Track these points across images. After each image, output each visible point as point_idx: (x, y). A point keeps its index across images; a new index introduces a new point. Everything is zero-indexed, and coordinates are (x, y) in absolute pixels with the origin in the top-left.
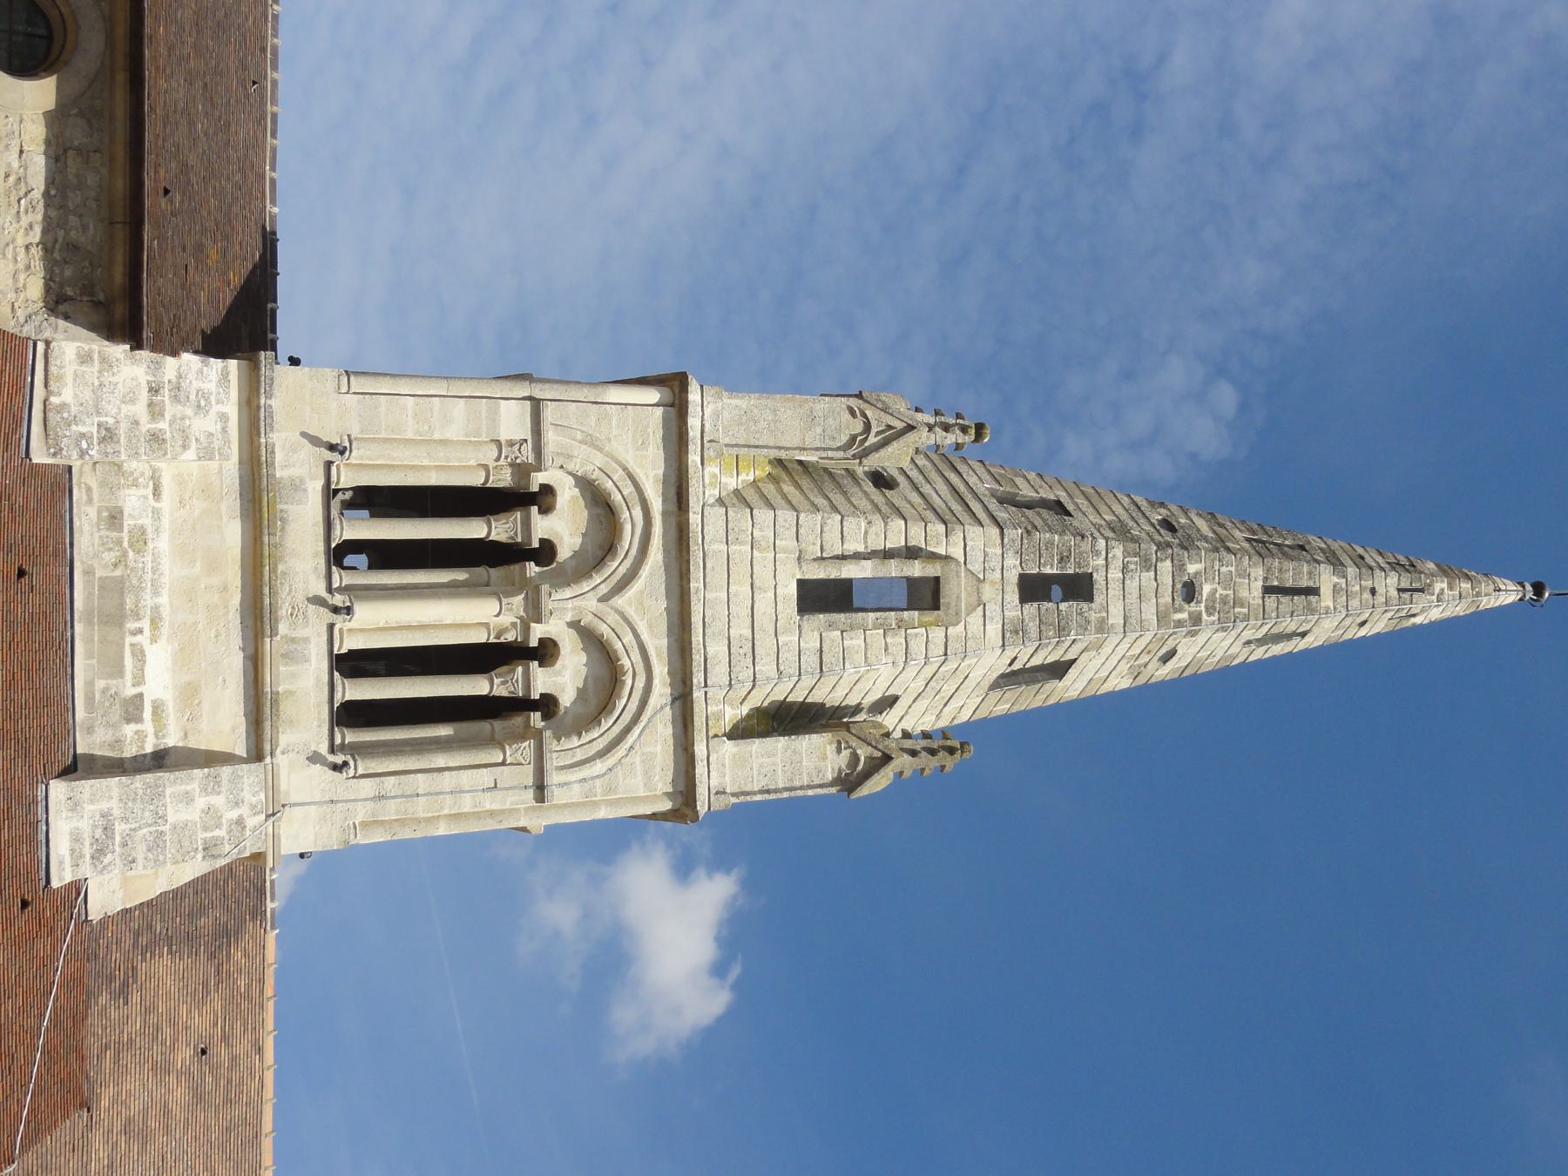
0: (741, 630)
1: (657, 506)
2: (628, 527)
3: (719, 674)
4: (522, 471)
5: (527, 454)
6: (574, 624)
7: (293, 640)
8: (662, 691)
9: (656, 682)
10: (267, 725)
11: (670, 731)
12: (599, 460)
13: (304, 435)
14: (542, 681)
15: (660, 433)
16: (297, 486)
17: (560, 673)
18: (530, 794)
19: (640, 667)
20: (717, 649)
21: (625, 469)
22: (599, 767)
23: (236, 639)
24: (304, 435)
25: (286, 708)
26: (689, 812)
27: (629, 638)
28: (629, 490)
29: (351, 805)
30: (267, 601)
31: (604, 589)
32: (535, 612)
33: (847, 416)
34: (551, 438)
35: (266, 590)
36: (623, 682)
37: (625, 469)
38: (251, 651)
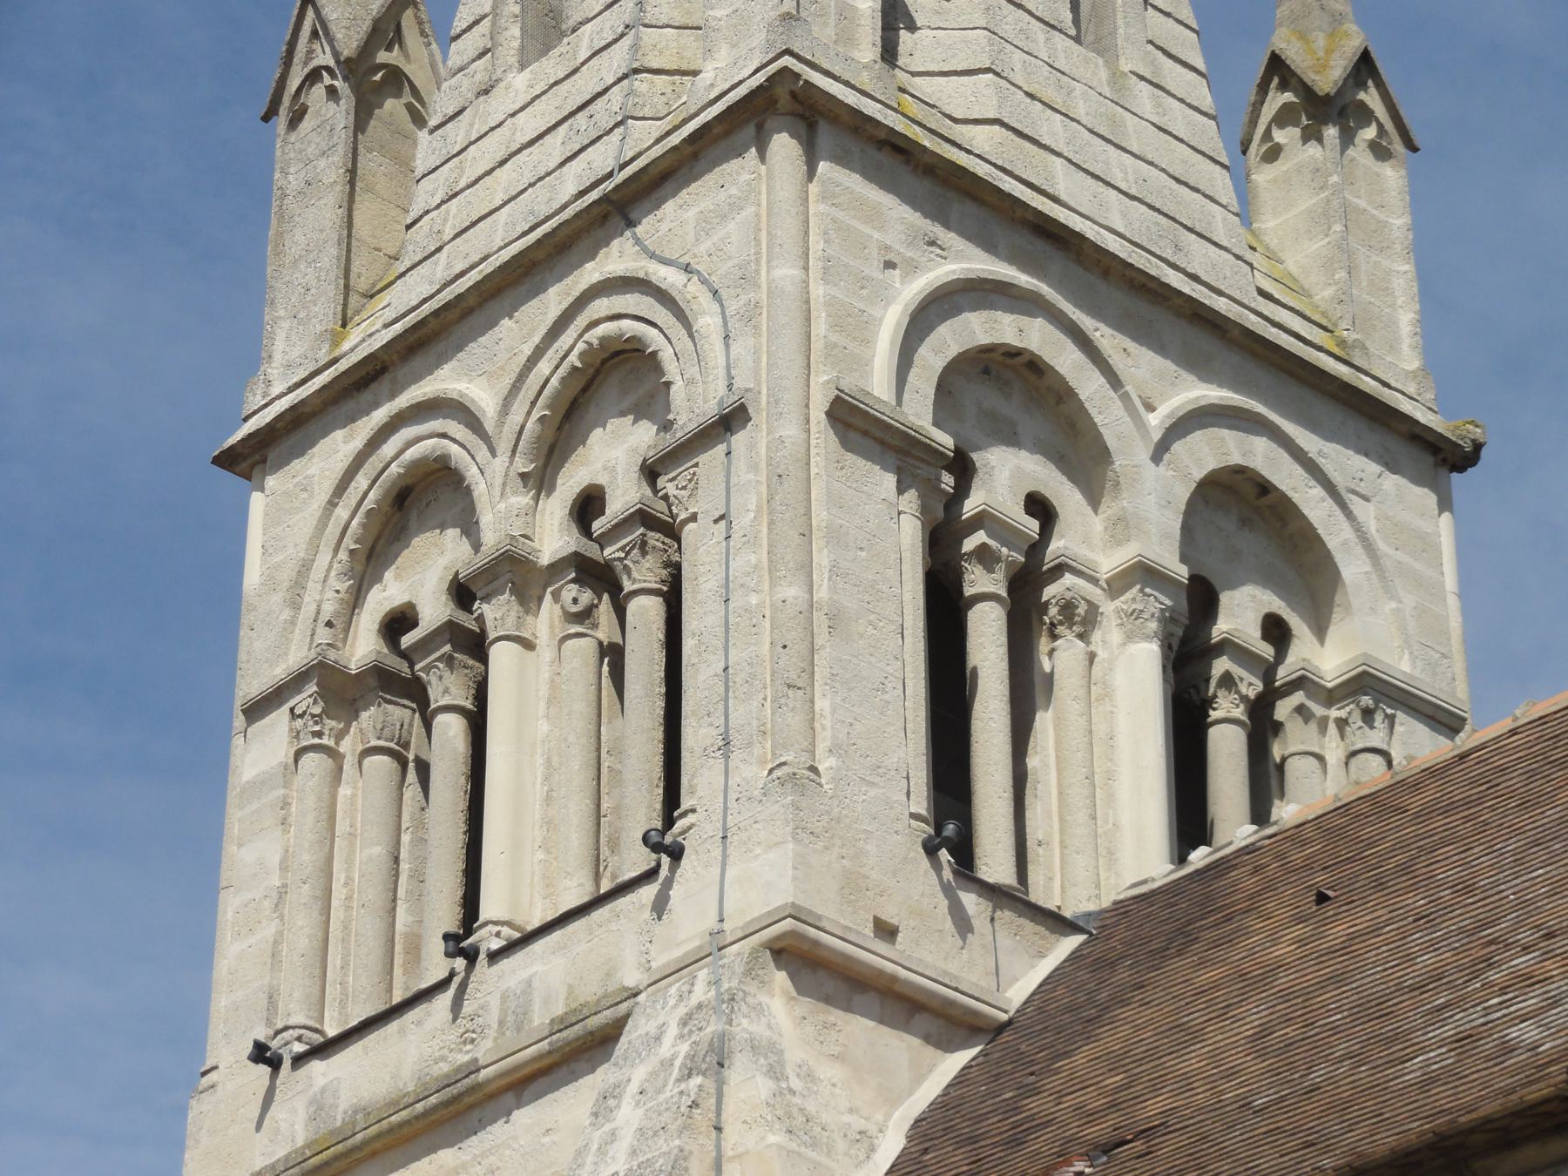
0: (555, 148)
1: (380, 415)
2: (412, 454)
3: (601, 158)
4: (341, 691)
5: (304, 699)
6: (541, 480)
7: (501, 1023)
8: (617, 258)
9: (596, 277)
10: (594, 1022)
11: (669, 207)
12: (324, 558)
13: (259, 1127)
14: (624, 496)
15: (296, 464)
16: (318, 1107)
17: (612, 471)
18: (739, 440)
19: (581, 321)
20: (570, 182)
21: (332, 504)
22: (708, 321)
23: (497, 1133)
24: (259, 1127)
25: (590, 991)
26: (782, 93)
27: (544, 367)
28: (361, 481)
29: (732, 796)
30: (433, 1100)
31: (482, 453)
32: (514, 572)
33: (307, 124)
34: (280, 672)
35: (419, 1107)
36: (604, 340)
37: (332, 504)
38: (509, 1098)
